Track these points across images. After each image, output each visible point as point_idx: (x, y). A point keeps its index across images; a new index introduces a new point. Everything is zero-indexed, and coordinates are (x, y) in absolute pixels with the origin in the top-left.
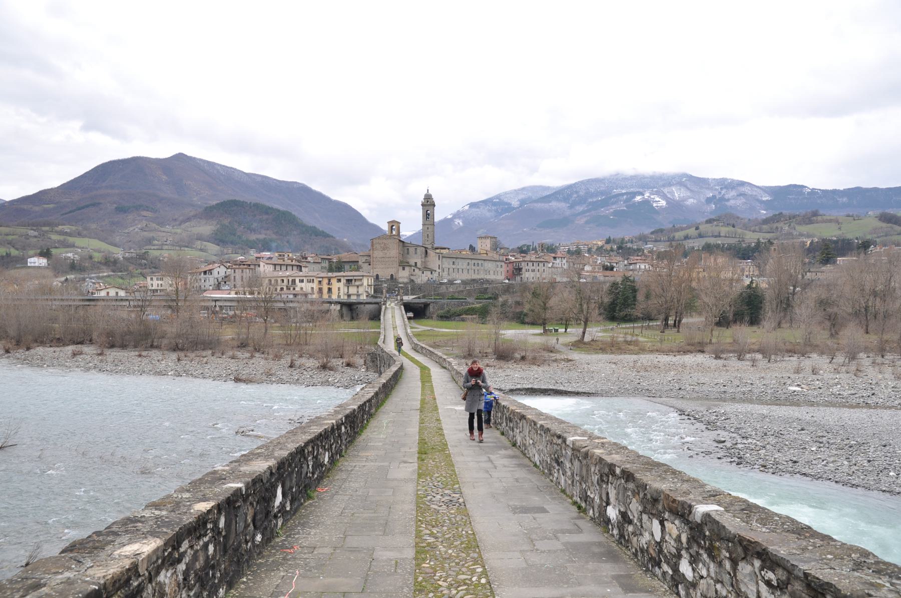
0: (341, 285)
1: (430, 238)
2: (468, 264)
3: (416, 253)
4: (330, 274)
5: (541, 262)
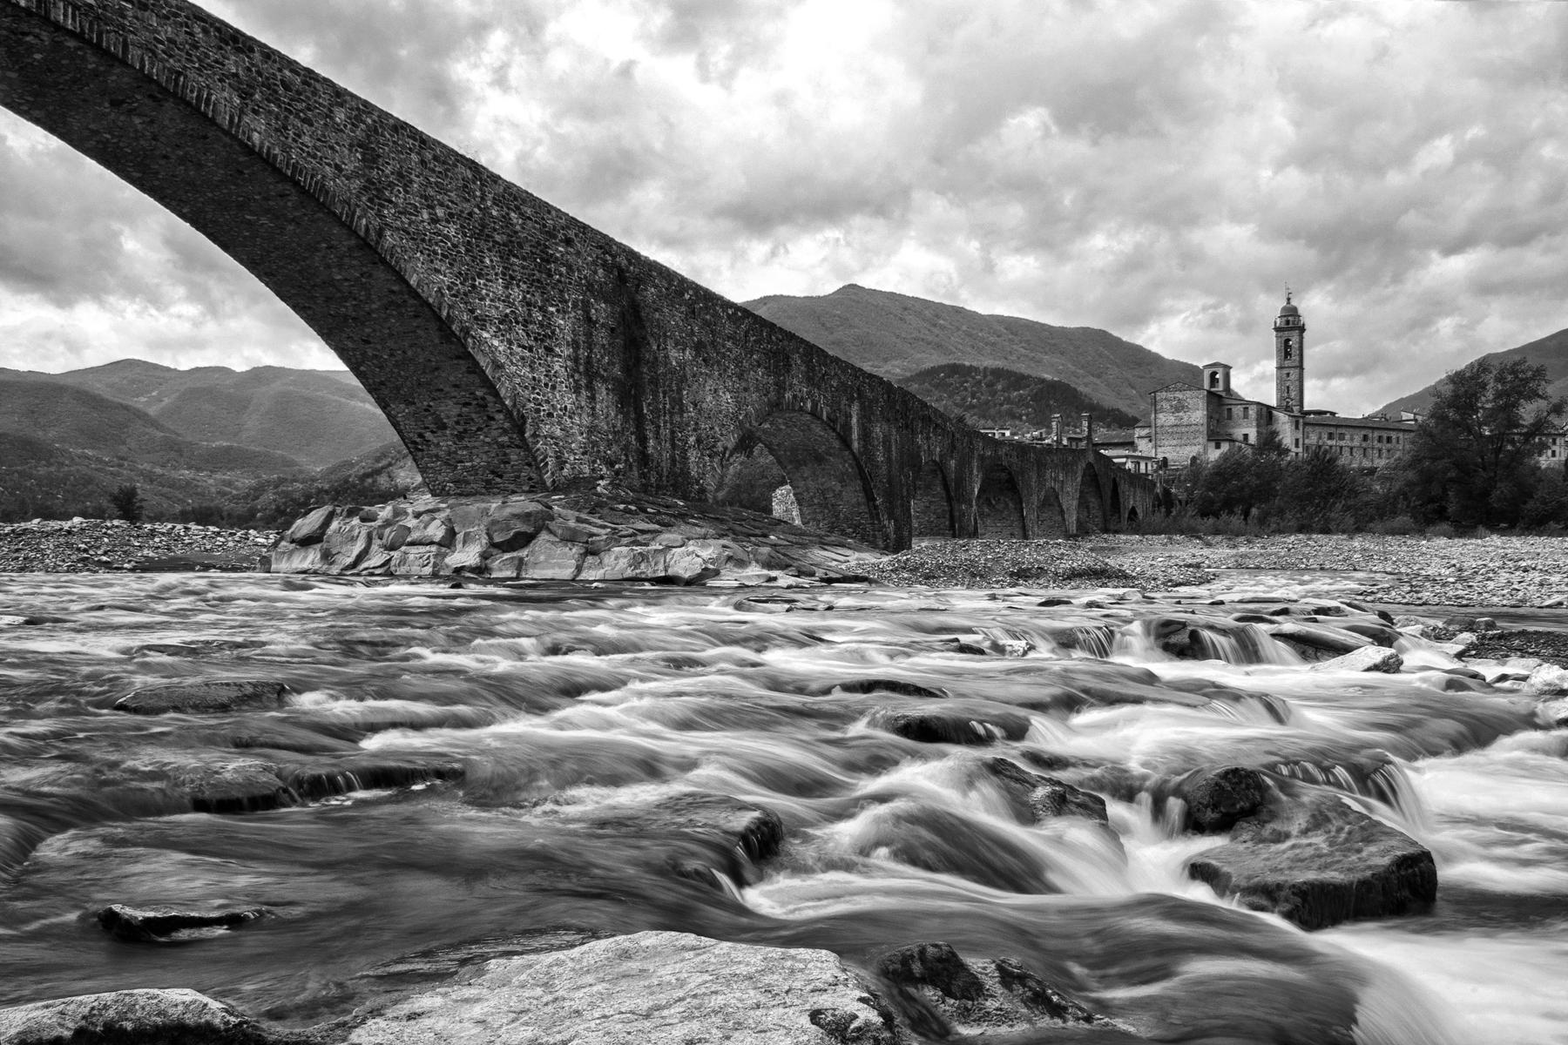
2: (1365, 438)
3: (1246, 416)
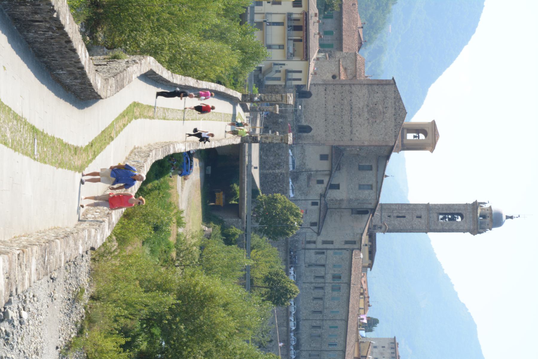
1: (396, 222)
3: (361, 187)
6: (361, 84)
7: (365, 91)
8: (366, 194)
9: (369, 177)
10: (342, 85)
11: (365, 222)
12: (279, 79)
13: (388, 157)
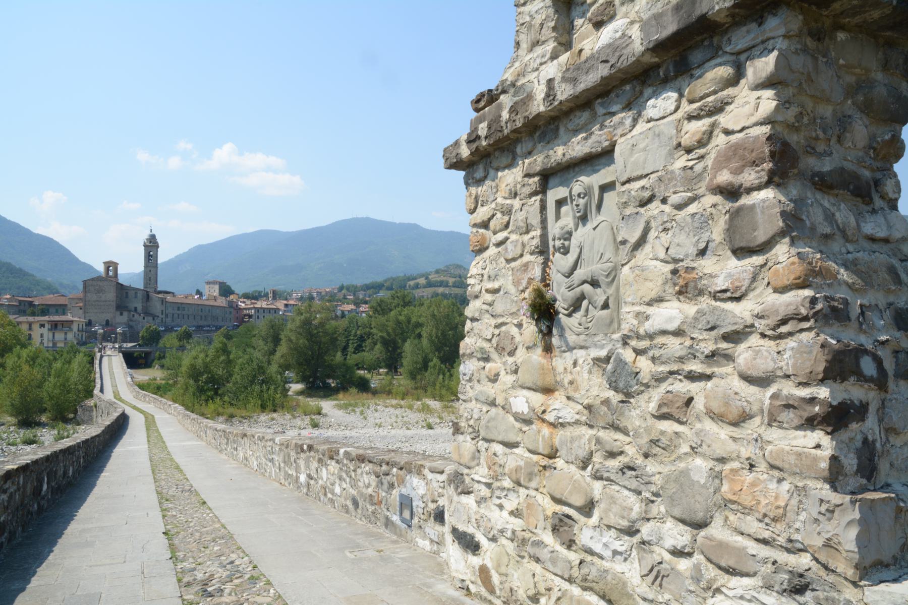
0: (45, 331)
1: (153, 281)
3: (136, 297)
4: (31, 319)
5: (273, 309)
6: (85, 296)
7: (88, 295)
8: (140, 295)
9: (131, 294)
10: (85, 305)
11: (154, 296)
12: (82, 335)
13: (122, 285)
